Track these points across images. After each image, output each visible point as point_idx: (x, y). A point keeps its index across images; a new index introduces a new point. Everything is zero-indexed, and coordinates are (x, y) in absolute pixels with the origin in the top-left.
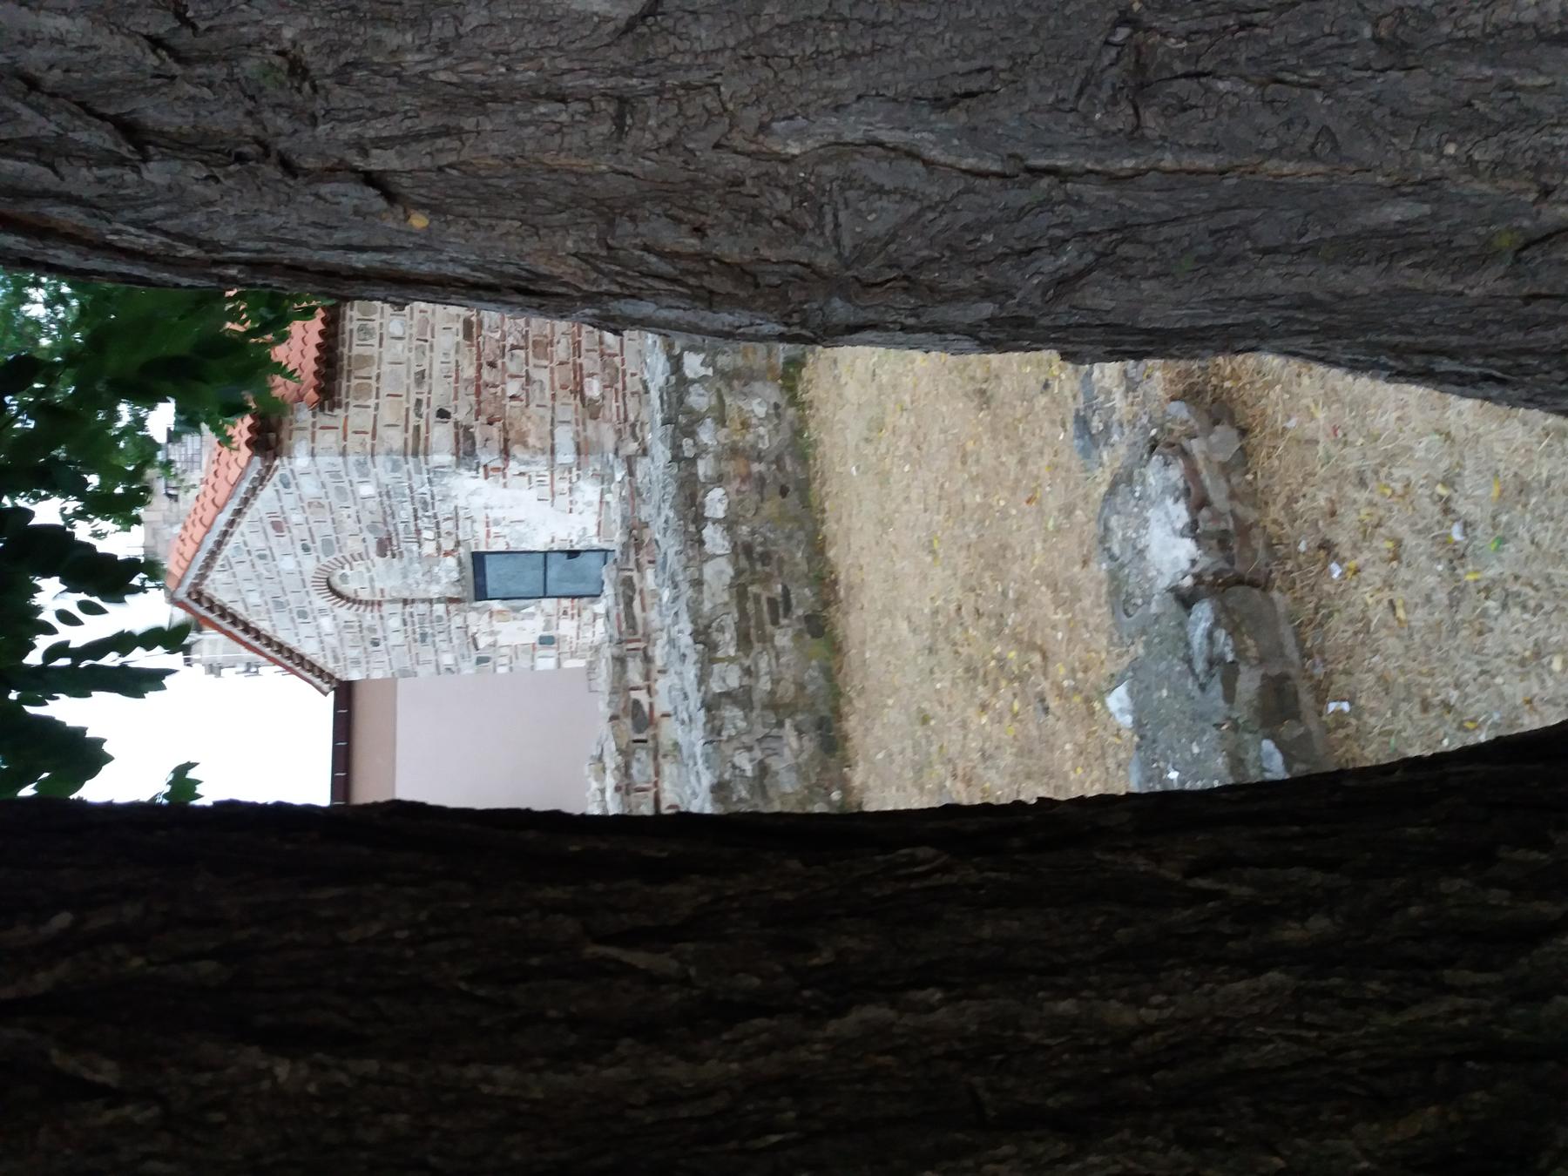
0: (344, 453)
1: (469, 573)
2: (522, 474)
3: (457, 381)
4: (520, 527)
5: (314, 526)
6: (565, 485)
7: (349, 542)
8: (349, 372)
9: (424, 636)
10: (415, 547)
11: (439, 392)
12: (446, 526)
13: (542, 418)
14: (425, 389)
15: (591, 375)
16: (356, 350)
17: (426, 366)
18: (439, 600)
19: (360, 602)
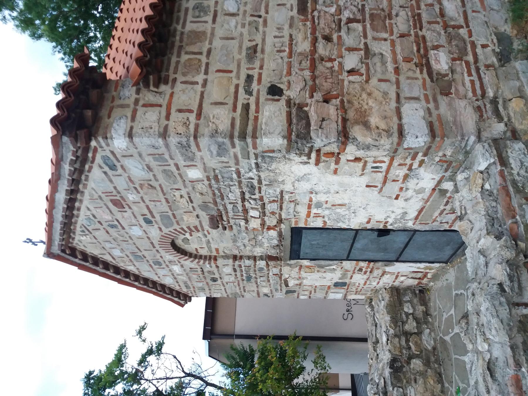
0: (164, 134)
1: (287, 242)
2: (357, 159)
3: (290, 56)
5: (151, 205)
6: (401, 172)
7: (185, 218)
8: (181, 47)
9: (249, 278)
10: (243, 223)
11: (271, 68)
13: (385, 94)
14: (257, 64)
15: (436, 48)
16: (190, 26)
17: (258, 40)
18: (261, 258)
19: (201, 257)
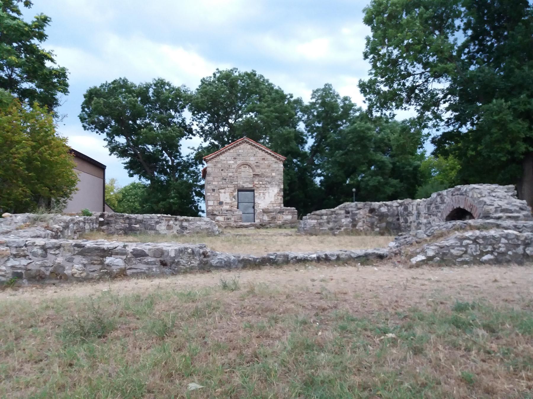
4: (263, 198)
12: (263, 186)
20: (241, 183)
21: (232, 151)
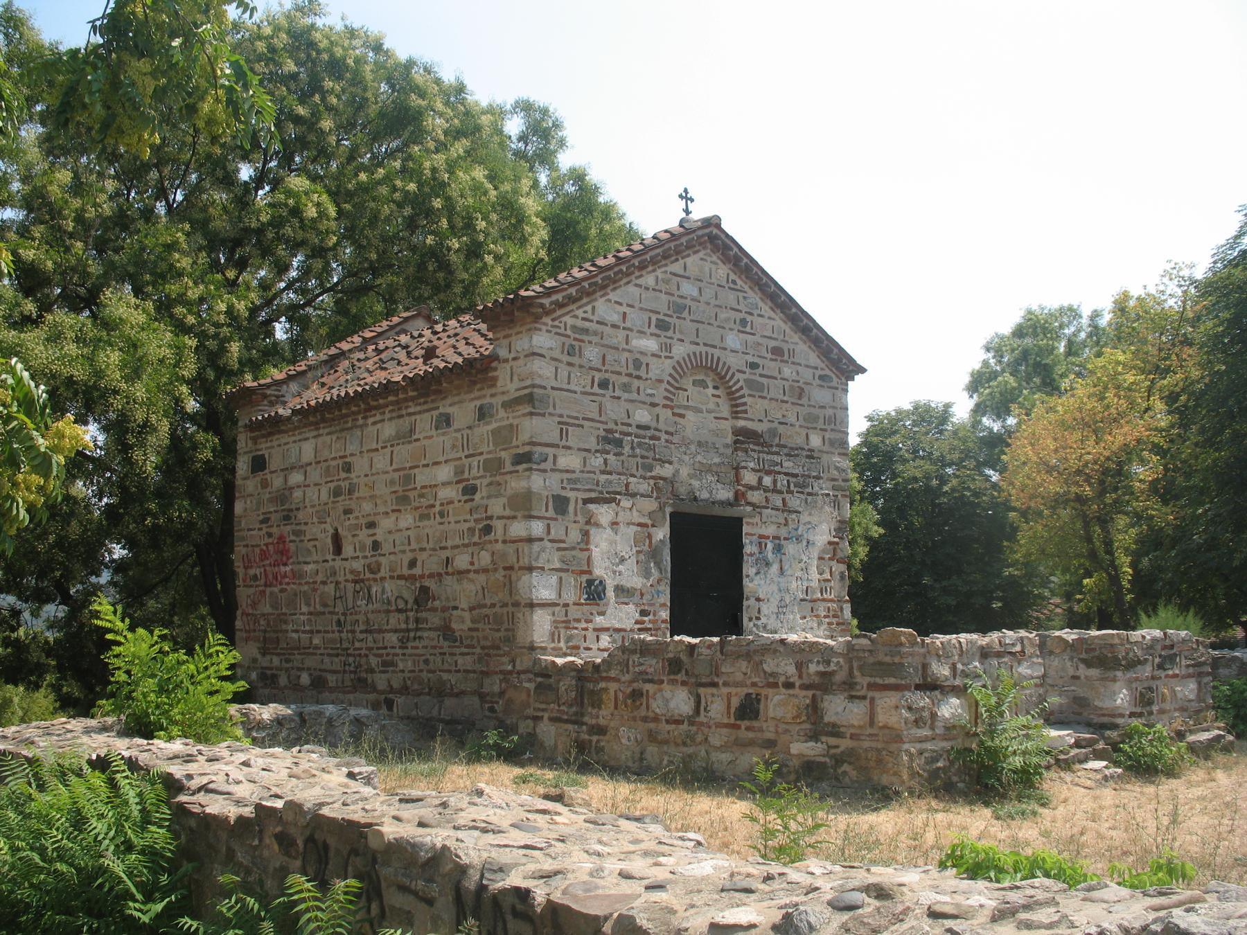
20: (684, 472)
21: (649, 280)
